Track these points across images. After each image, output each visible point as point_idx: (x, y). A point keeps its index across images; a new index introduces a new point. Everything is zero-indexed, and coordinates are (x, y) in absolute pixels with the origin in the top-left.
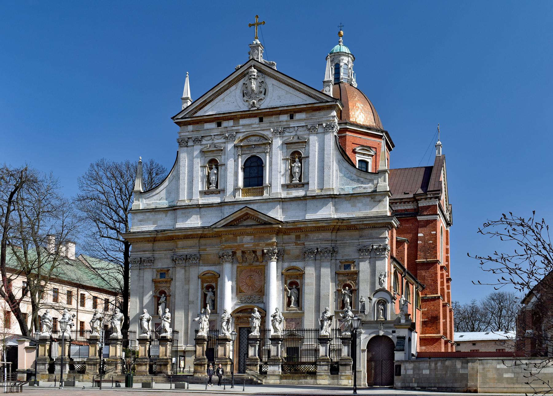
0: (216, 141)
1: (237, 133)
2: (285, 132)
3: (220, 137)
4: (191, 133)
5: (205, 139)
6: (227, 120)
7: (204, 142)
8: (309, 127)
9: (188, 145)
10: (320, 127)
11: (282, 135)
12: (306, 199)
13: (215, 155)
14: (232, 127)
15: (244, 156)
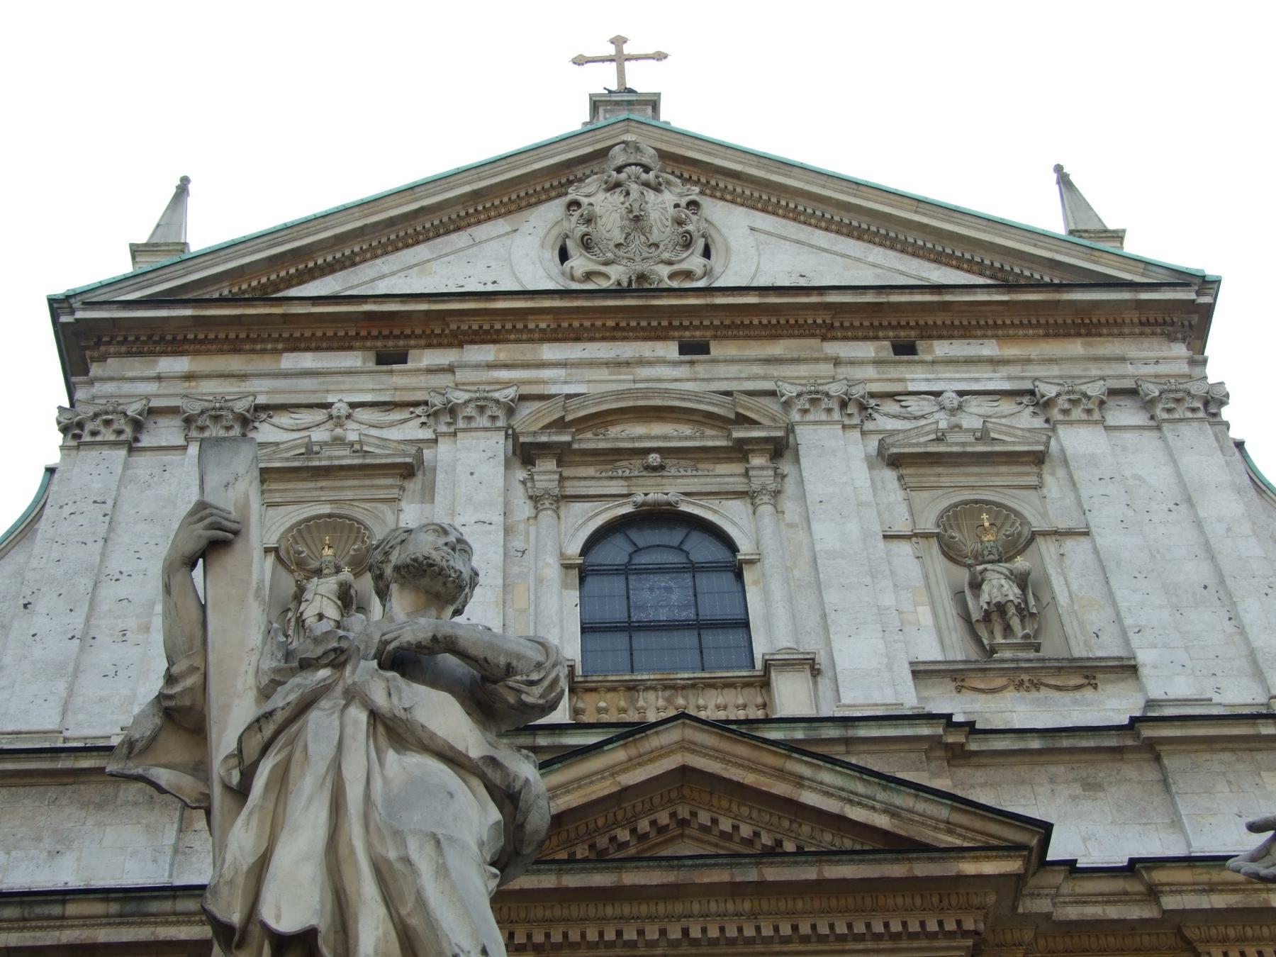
0: (352, 436)
1: (528, 404)
2: (875, 415)
3: (396, 415)
4: (182, 387)
5: (276, 420)
6: (450, 345)
7: (266, 432)
8: (1050, 391)
9: (139, 445)
10: (1111, 403)
11: (856, 421)
12: (1153, 751)
13: (349, 495)
14: (490, 366)
15: (578, 507)
